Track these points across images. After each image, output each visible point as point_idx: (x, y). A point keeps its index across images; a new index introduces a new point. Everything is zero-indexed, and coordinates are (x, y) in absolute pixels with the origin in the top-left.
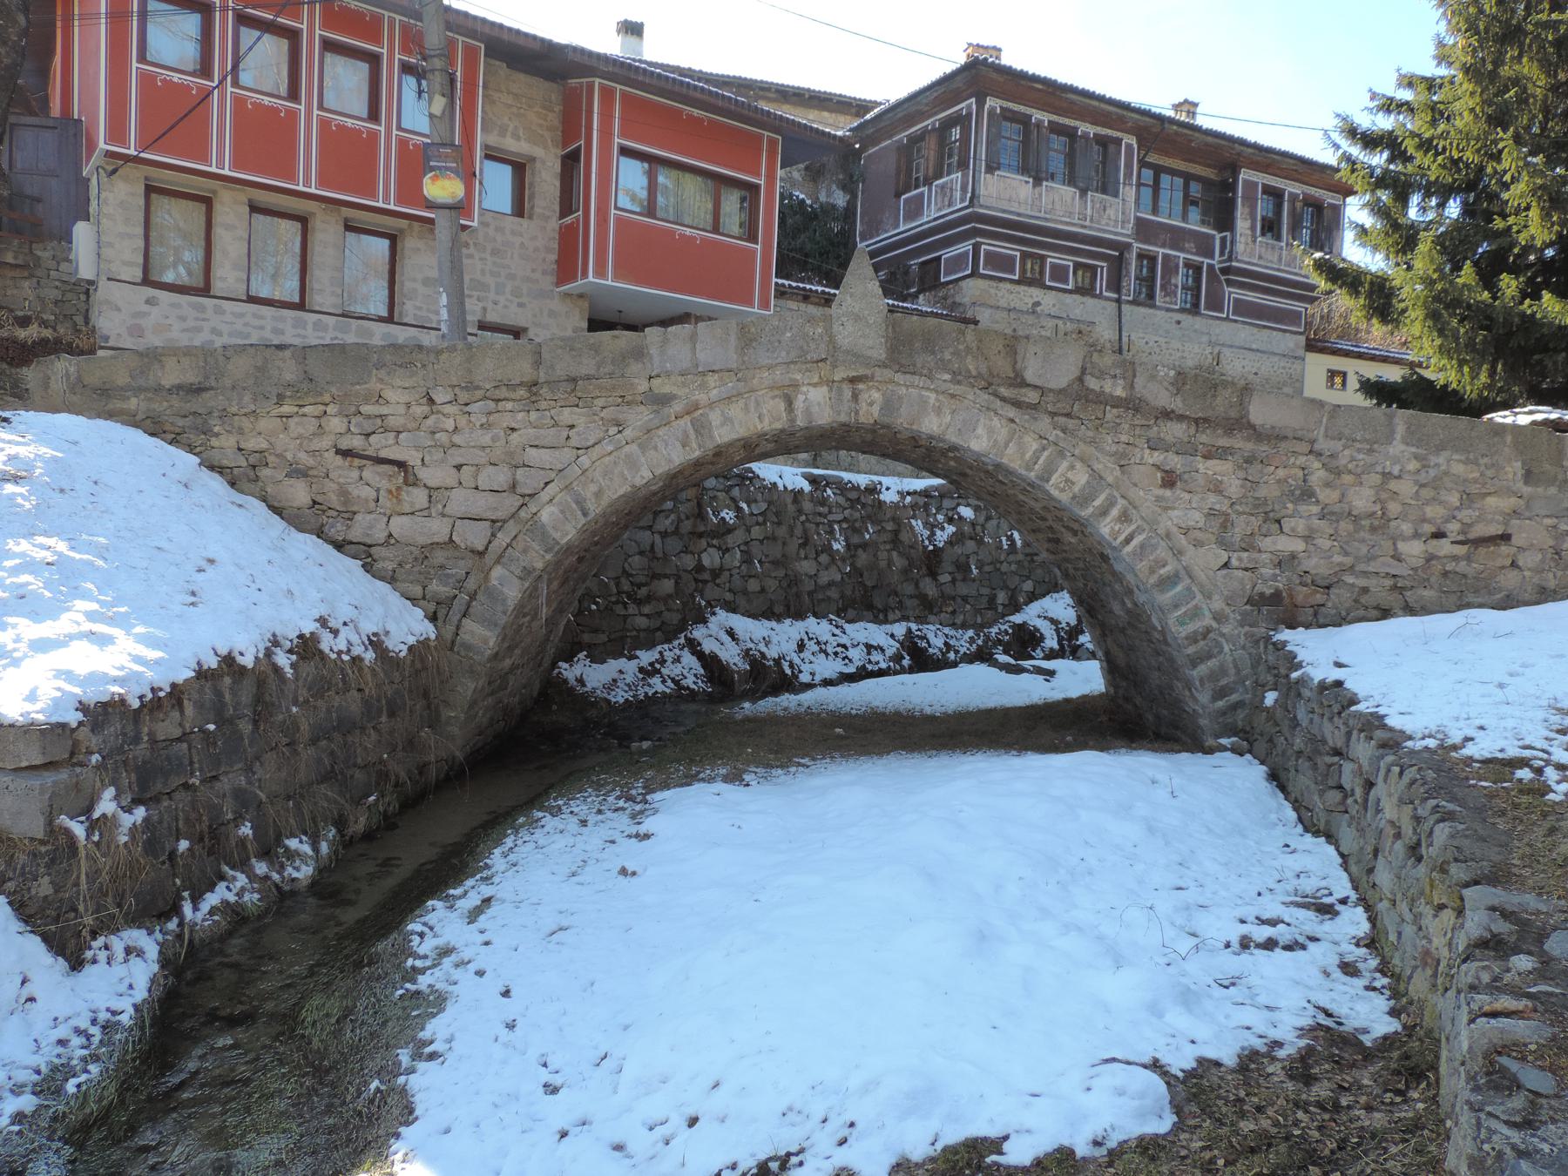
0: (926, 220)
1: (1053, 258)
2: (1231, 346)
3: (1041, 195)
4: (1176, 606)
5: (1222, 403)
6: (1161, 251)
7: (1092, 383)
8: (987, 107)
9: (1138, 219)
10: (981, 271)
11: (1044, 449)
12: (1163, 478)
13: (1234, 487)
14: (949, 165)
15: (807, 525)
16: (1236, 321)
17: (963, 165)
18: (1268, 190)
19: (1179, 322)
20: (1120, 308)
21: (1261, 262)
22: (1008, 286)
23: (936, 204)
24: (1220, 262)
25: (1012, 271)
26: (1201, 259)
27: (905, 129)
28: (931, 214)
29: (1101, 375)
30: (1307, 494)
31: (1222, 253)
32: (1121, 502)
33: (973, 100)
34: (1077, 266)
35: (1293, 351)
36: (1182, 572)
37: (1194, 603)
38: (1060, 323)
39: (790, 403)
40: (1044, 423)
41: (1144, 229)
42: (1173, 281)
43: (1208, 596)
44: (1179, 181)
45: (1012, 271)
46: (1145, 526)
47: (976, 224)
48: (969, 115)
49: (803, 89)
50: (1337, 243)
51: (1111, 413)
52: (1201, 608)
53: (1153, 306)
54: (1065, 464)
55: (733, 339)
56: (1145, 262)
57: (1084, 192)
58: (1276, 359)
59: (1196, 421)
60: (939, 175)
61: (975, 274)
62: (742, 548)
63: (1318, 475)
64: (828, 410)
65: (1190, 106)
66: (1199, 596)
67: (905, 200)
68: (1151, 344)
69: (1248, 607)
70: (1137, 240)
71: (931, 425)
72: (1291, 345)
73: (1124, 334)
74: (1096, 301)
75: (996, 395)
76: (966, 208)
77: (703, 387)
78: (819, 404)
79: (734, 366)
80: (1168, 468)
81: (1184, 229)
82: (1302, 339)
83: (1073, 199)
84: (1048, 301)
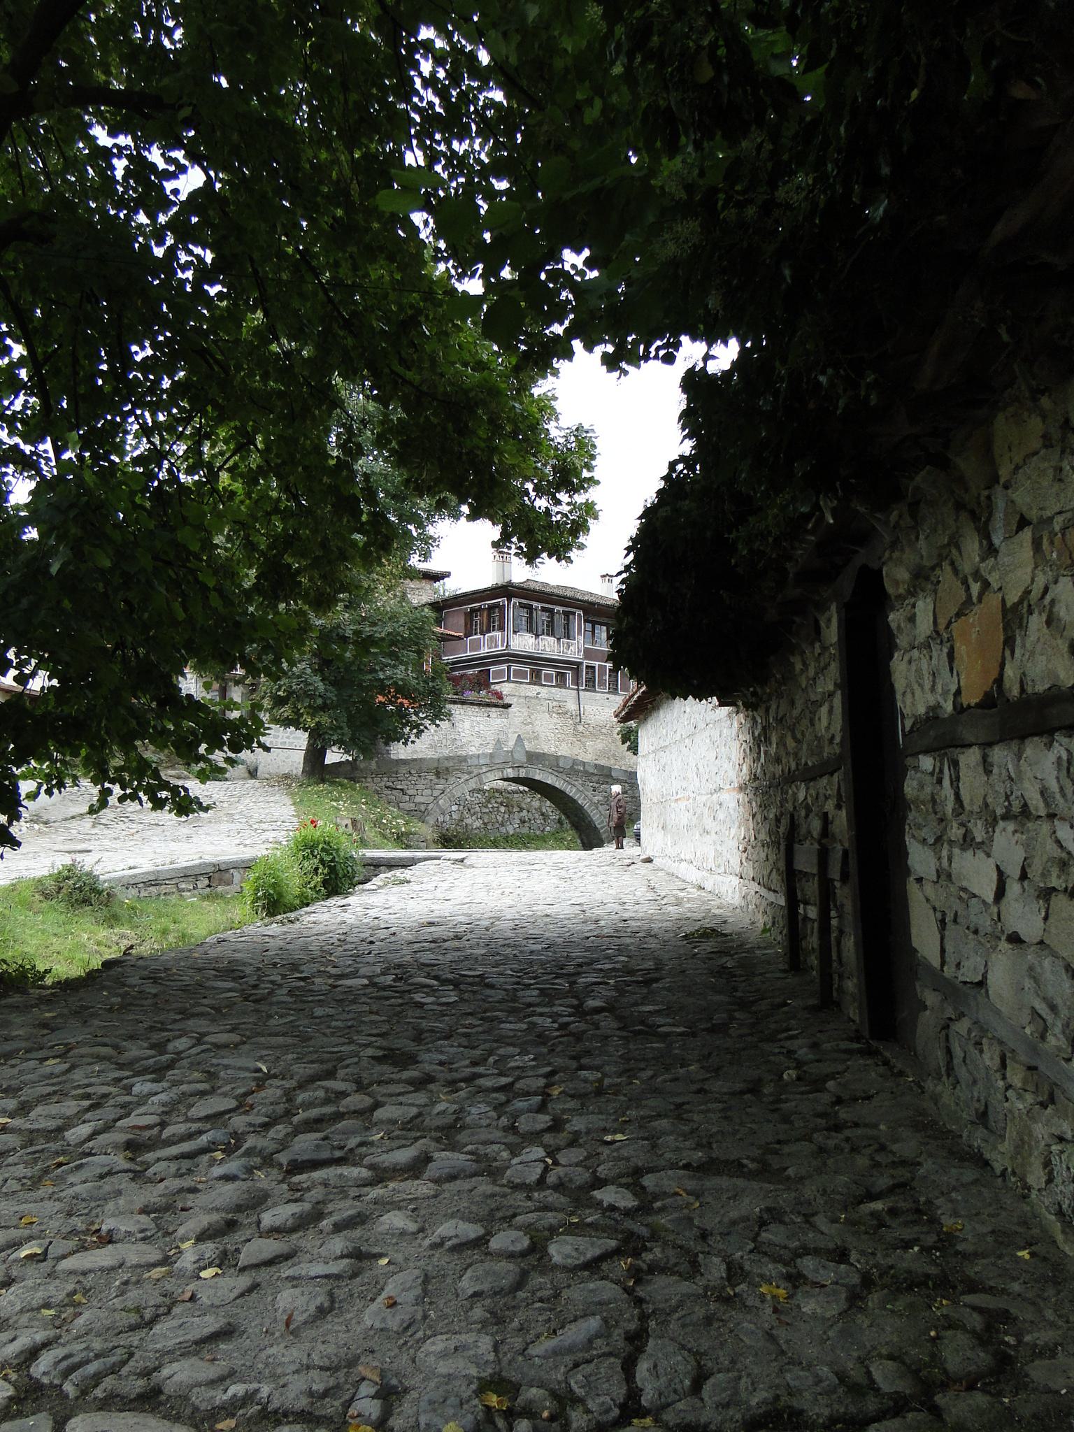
1: (545, 671)
5: (605, 772)
28: (484, 651)
34: (558, 673)
41: (588, 654)
44: (604, 628)
47: (511, 658)
57: (559, 639)
60: (489, 632)
61: (508, 681)
71: (537, 777)
84: (544, 692)
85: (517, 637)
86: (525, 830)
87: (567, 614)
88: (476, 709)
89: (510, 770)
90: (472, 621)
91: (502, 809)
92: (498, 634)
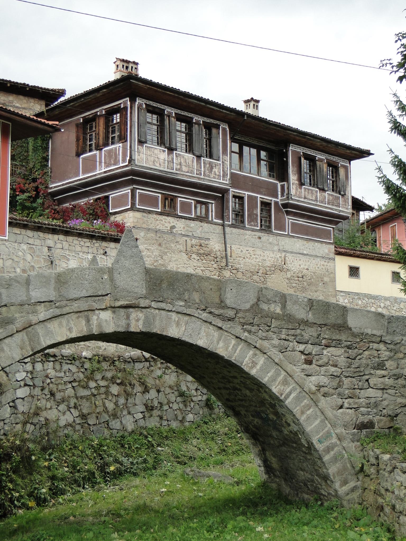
0: (98, 172)
1: (181, 199)
2: (292, 252)
3: (173, 159)
4: (318, 432)
6: (247, 193)
7: (265, 307)
8: (137, 103)
9: (232, 174)
10: (138, 207)
11: (239, 344)
12: (305, 360)
13: (342, 361)
14: (113, 138)
15: (51, 385)
16: (293, 237)
17: (123, 138)
18: (307, 157)
19: (260, 238)
20: (224, 229)
21: (306, 200)
22: (155, 216)
23: (105, 163)
24: (281, 200)
25: (157, 206)
26: (270, 198)
27: (81, 113)
29: (268, 301)
30: (381, 366)
31: (282, 195)
32: (283, 373)
33: (128, 99)
35: (328, 254)
36: (319, 413)
37: (326, 429)
38: (188, 239)
39: (88, 320)
40: (238, 330)
42: (255, 212)
43: (334, 426)
44: (254, 151)
45: (157, 206)
46: (298, 387)
48: (126, 108)
49: (6, 81)
50: (348, 189)
51: (274, 323)
52: (330, 433)
53: (244, 228)
54: (251, 352)
55: (53, 281)
56: (237, 200)
58: (319, 259)
59: (320, 325)
60: (106, 145)
61: (133, 208)
62: (11, 404)
63: (385, 354)
64: (112, 325)
65: (254, 102)
66: (329, 425)
67: (83, 159)
68: (244, 252)
69: (355, 430)
70: (233, 187)
72: (327, 251)
73: (228, 246)
74: (210, 225)
75: (210, 313)
76: (126, 166)
77: (35, 312)
78: (106, 321)
79: (54, 299)
80: (307, 353)
81: (259, 179)
82: (333, 247)
83: (193, 162)
84: (180, 225)
85: (143, 149)
86: (153, 423)
87: (208, 127)
88: (86, 242)
89: (106, 315)
90: (85, 133)
91: (115, 389)
92: (119, 146)
